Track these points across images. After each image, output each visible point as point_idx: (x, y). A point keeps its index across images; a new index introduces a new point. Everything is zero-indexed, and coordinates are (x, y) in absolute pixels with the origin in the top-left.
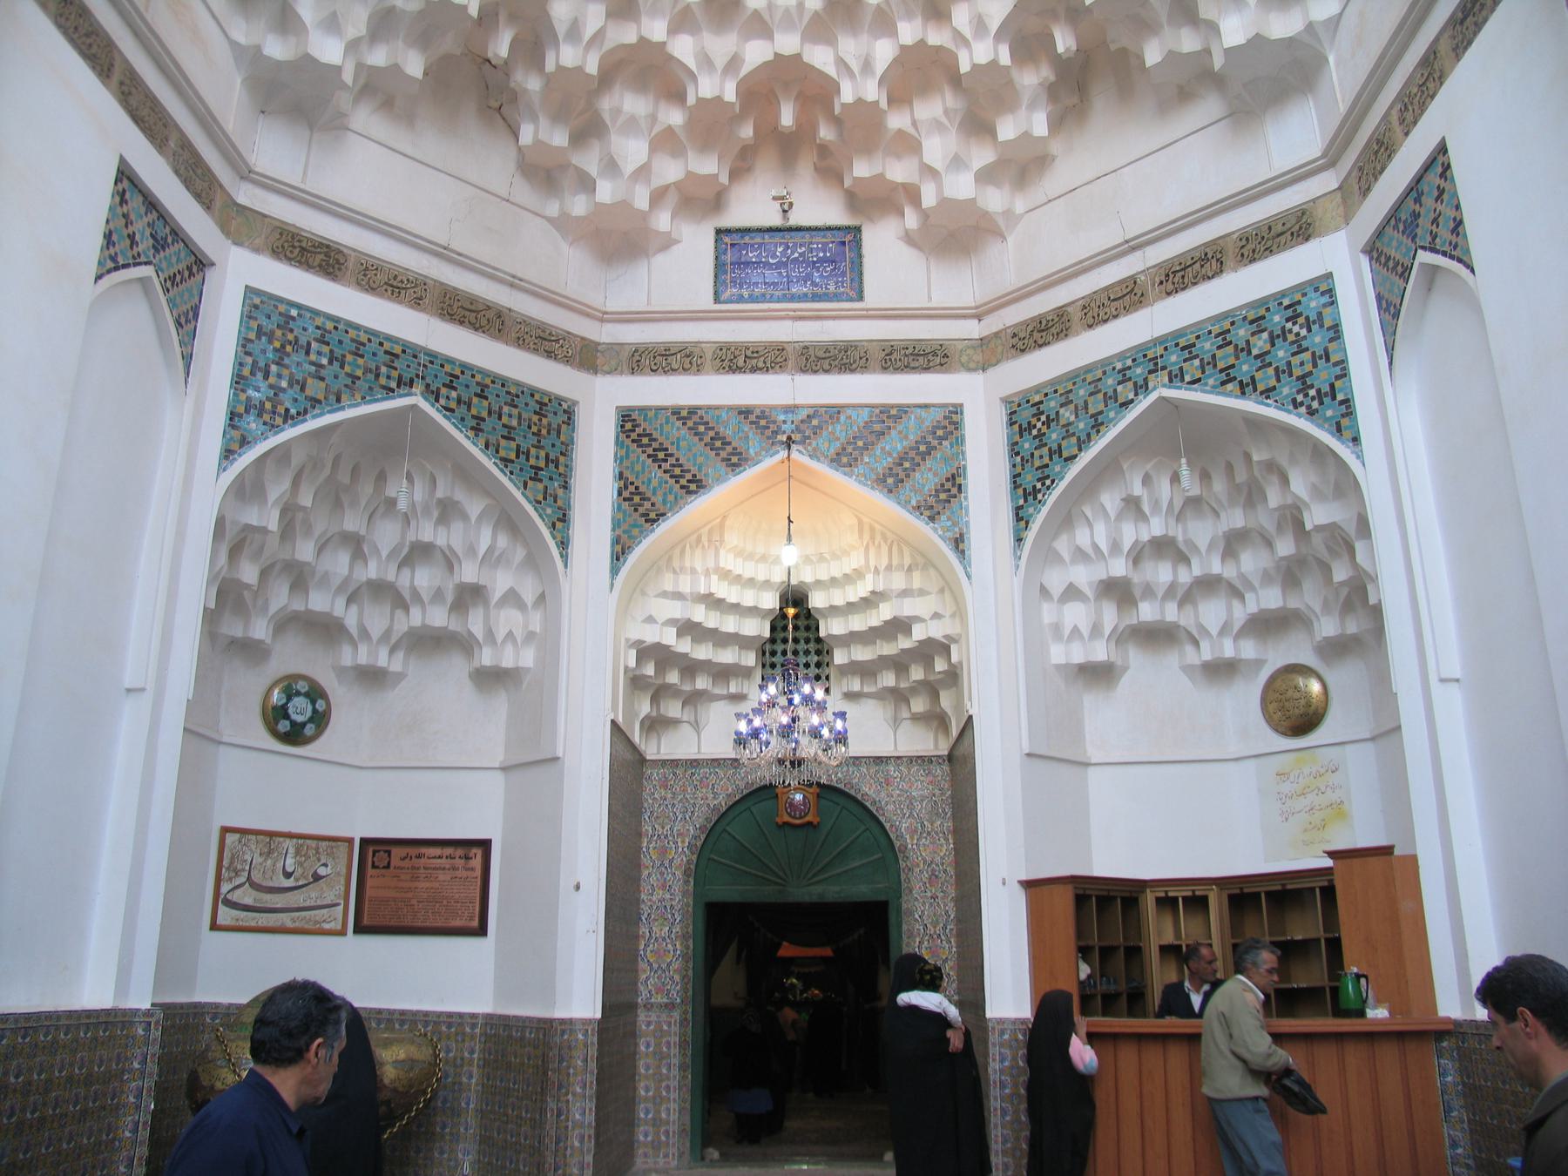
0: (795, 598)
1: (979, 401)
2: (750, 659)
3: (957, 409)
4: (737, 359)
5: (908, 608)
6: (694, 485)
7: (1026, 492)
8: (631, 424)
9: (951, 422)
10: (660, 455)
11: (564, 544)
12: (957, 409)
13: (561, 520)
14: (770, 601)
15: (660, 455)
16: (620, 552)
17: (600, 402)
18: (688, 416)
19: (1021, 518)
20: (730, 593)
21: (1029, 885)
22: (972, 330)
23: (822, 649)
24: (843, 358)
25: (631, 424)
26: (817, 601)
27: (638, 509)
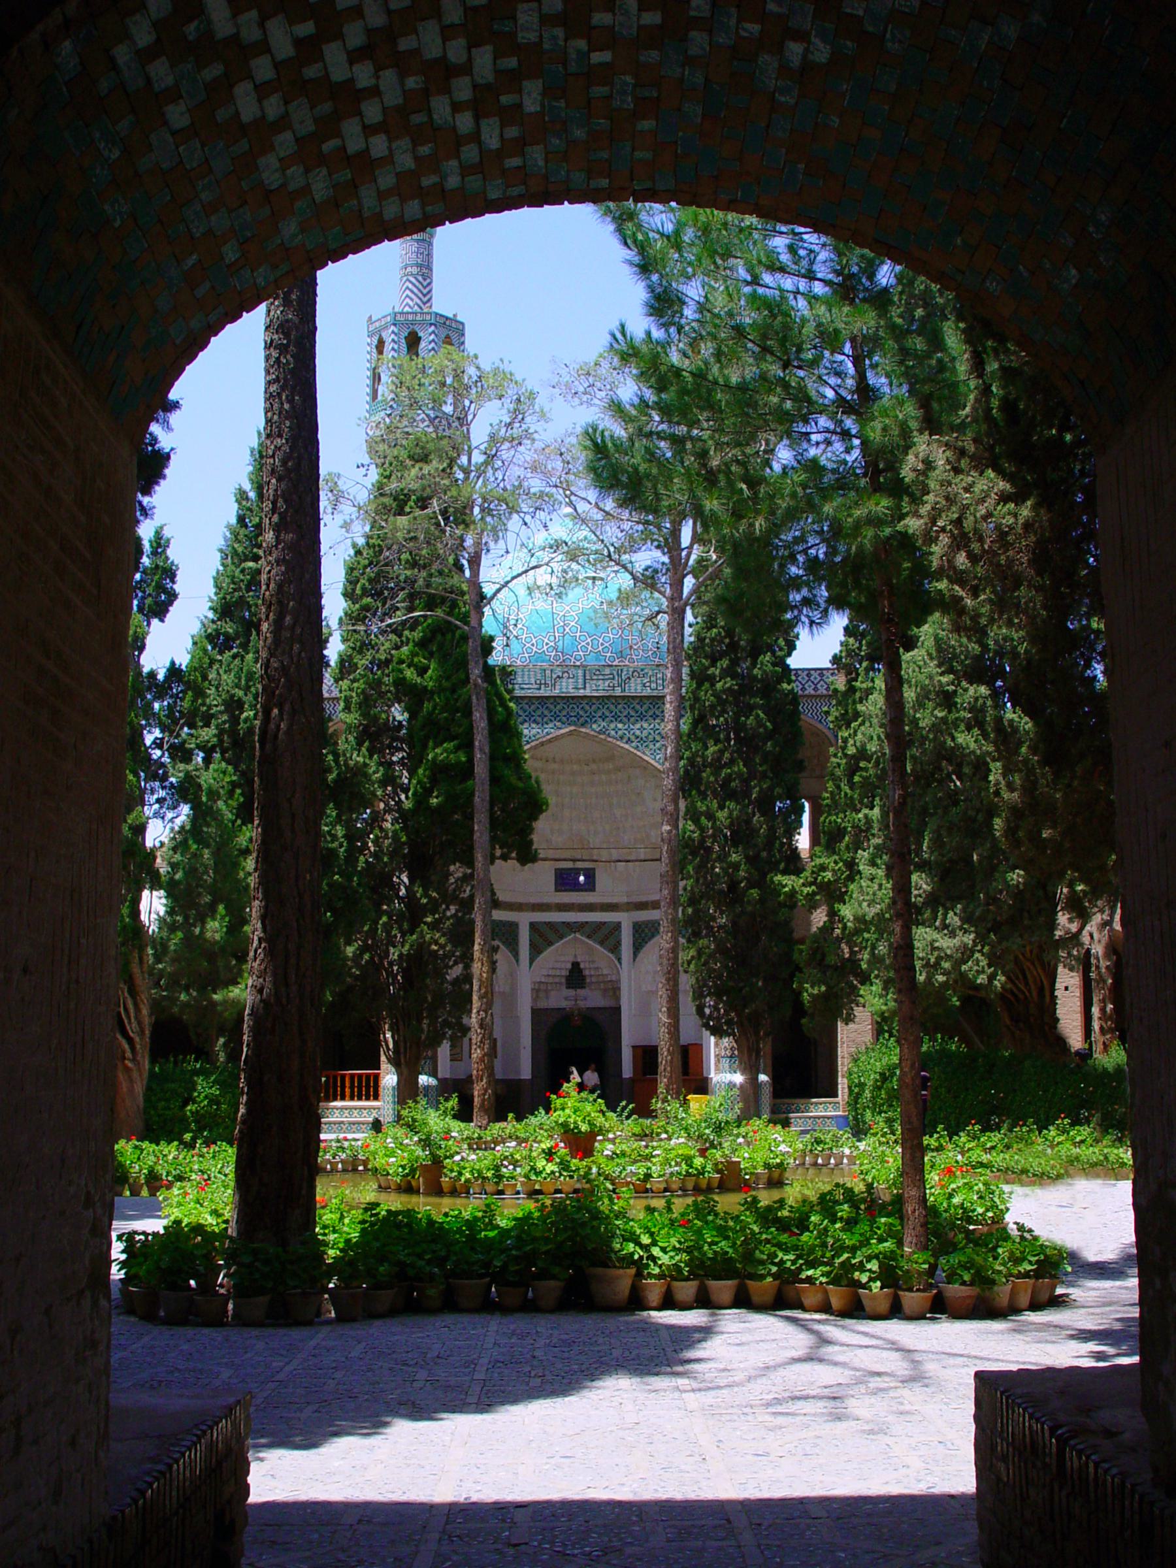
0: (576, 965)
1: (626, 920)
2: (563, 980)
3: (620, 923)
4: (562, 908)
5: (605, 972)
6: (550, 944)
7: (637, 948)
8: (533, 926)
9: (619, 925)
10: (541, 935)
11: (517, 961)
12: (620, 923)
13: (516, 955)
14: (569, 966)
15: (541, 935)
16: (532, 961)
17: (524, 920)
18: (549, 924)
19: (635, 955)
20: (558, 965)
21: (633, 1047)
22: (625, 900)
23: (583, 978)
24: (590, 908)
25: (533, 926)
26: (582, 966)
27: (536, 950)
